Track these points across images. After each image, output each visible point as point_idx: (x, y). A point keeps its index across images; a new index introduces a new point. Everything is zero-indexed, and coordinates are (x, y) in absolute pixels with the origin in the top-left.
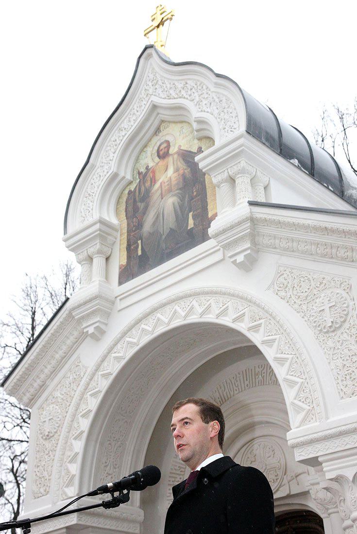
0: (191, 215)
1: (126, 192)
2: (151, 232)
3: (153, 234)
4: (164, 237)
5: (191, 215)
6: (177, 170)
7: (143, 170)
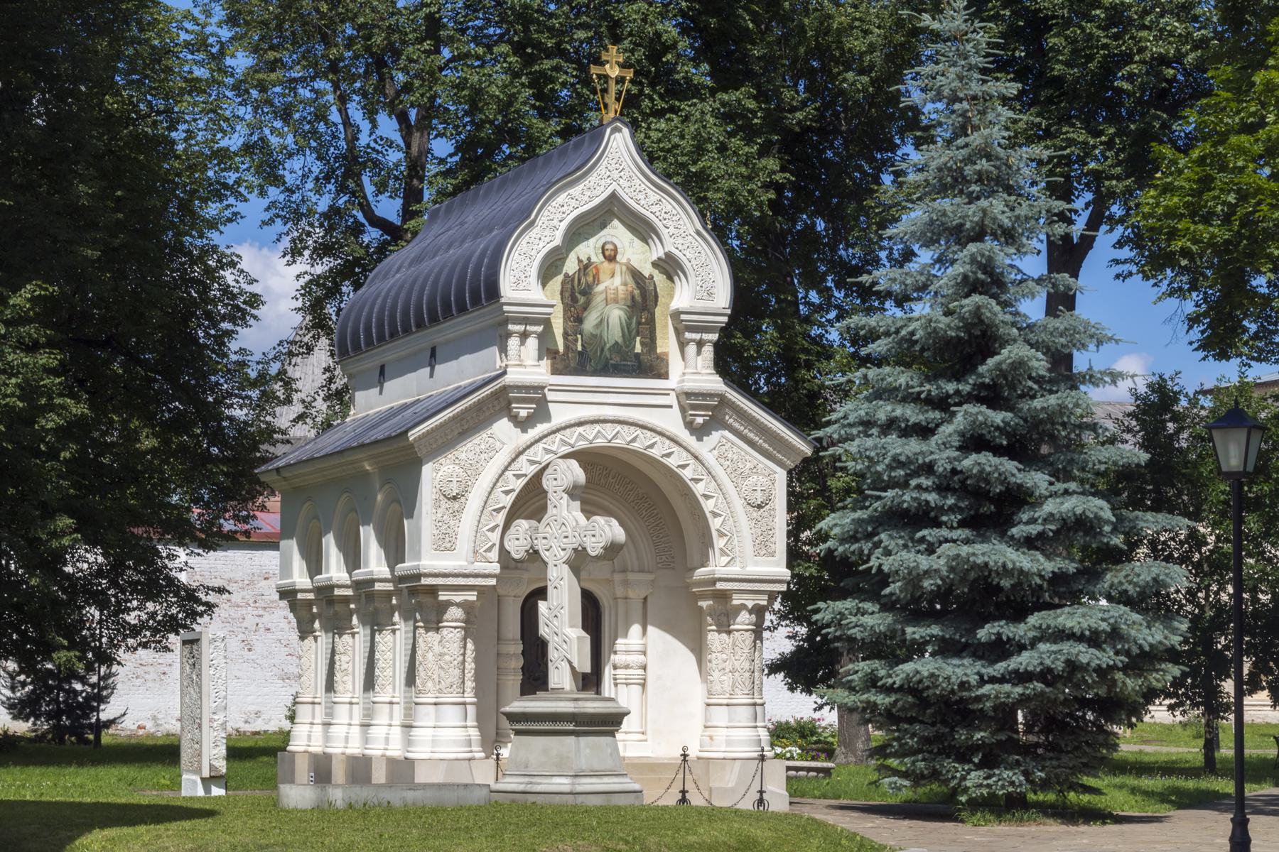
0: (638, 339)
3: (596, 339)
5: (638, 339)
6: (625, 284)
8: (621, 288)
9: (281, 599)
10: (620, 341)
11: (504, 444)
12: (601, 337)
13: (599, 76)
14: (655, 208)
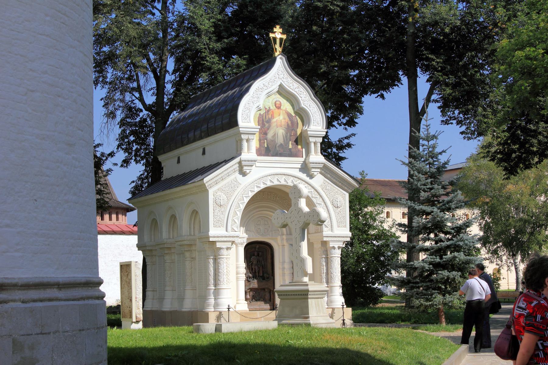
0: (290, 142)
1: (259, 112)
2: (272, 139)
3: (273, 141)
4: (278, 145)
5: (290, 142)
6: (285, 119)
7: (268, 109)
8: (283, 120)
9: (138, 250)
10: (282, 142)
11: (240, 184)
12: (275, 141)
13: (273, 38)
14: (297, 90)
